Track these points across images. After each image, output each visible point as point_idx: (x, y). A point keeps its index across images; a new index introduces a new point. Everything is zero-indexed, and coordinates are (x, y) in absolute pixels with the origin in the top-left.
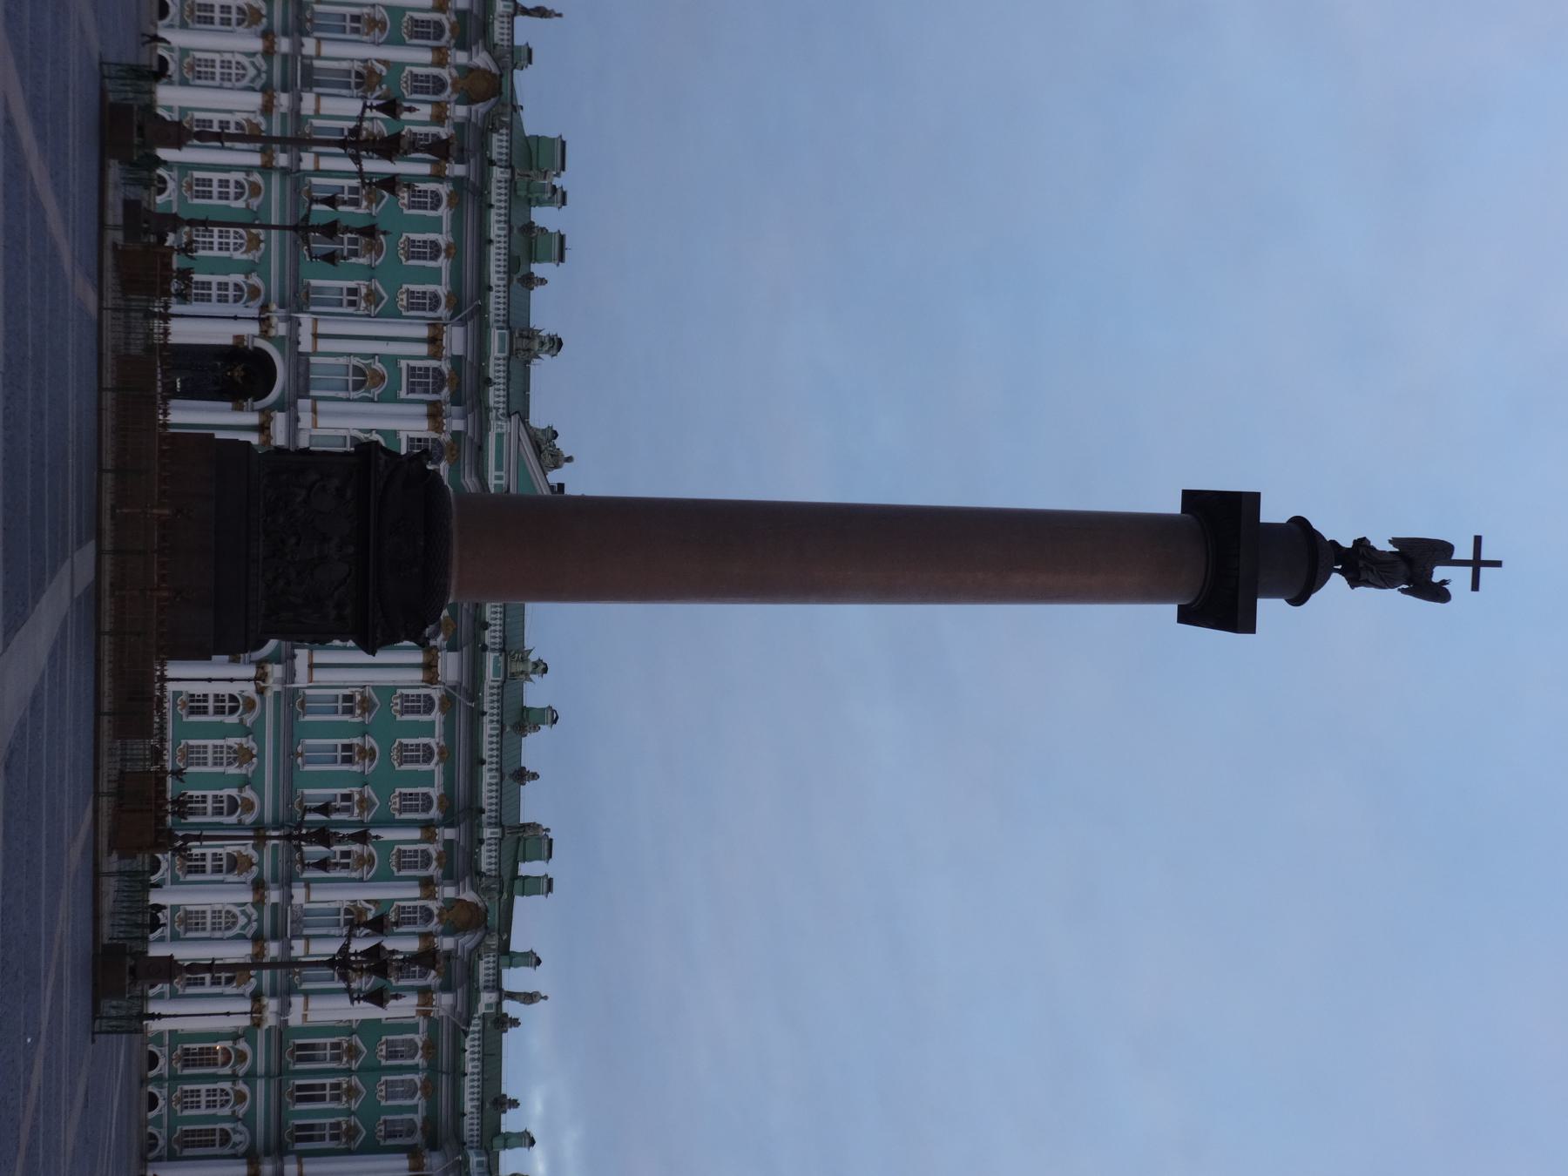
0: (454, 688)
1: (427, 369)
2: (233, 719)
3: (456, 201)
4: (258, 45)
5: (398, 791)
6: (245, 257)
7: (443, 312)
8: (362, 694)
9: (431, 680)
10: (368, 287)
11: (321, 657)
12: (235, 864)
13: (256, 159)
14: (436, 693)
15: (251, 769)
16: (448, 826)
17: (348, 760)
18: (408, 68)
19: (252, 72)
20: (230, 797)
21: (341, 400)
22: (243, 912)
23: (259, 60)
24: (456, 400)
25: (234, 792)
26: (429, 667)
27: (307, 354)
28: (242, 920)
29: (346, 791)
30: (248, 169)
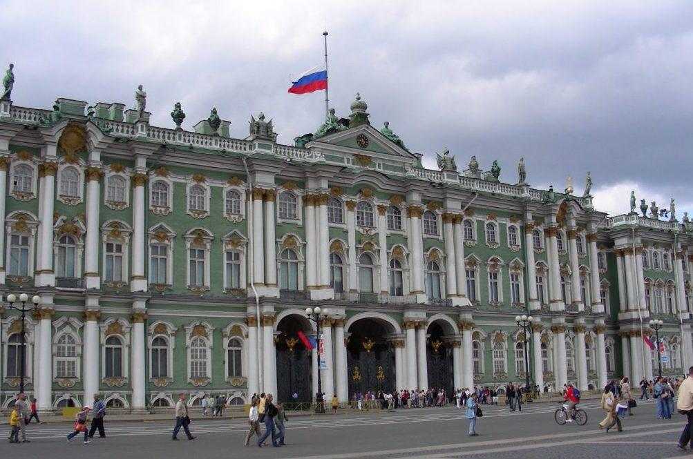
0: (463, 207)
2: (482, 344)
4: (45, 324)
6: (211, 338)
7: (242, 189)
10: (227, 244)
11: (453, 291)
13: (139, 327)
14: (465, 218)
18: (58, 198)
19: (67, 329)
21: (305, 267)
23: (58, 323)
24: (302, 185)
27: (281, 291)
28: (568, 339)
30: (146, 334)
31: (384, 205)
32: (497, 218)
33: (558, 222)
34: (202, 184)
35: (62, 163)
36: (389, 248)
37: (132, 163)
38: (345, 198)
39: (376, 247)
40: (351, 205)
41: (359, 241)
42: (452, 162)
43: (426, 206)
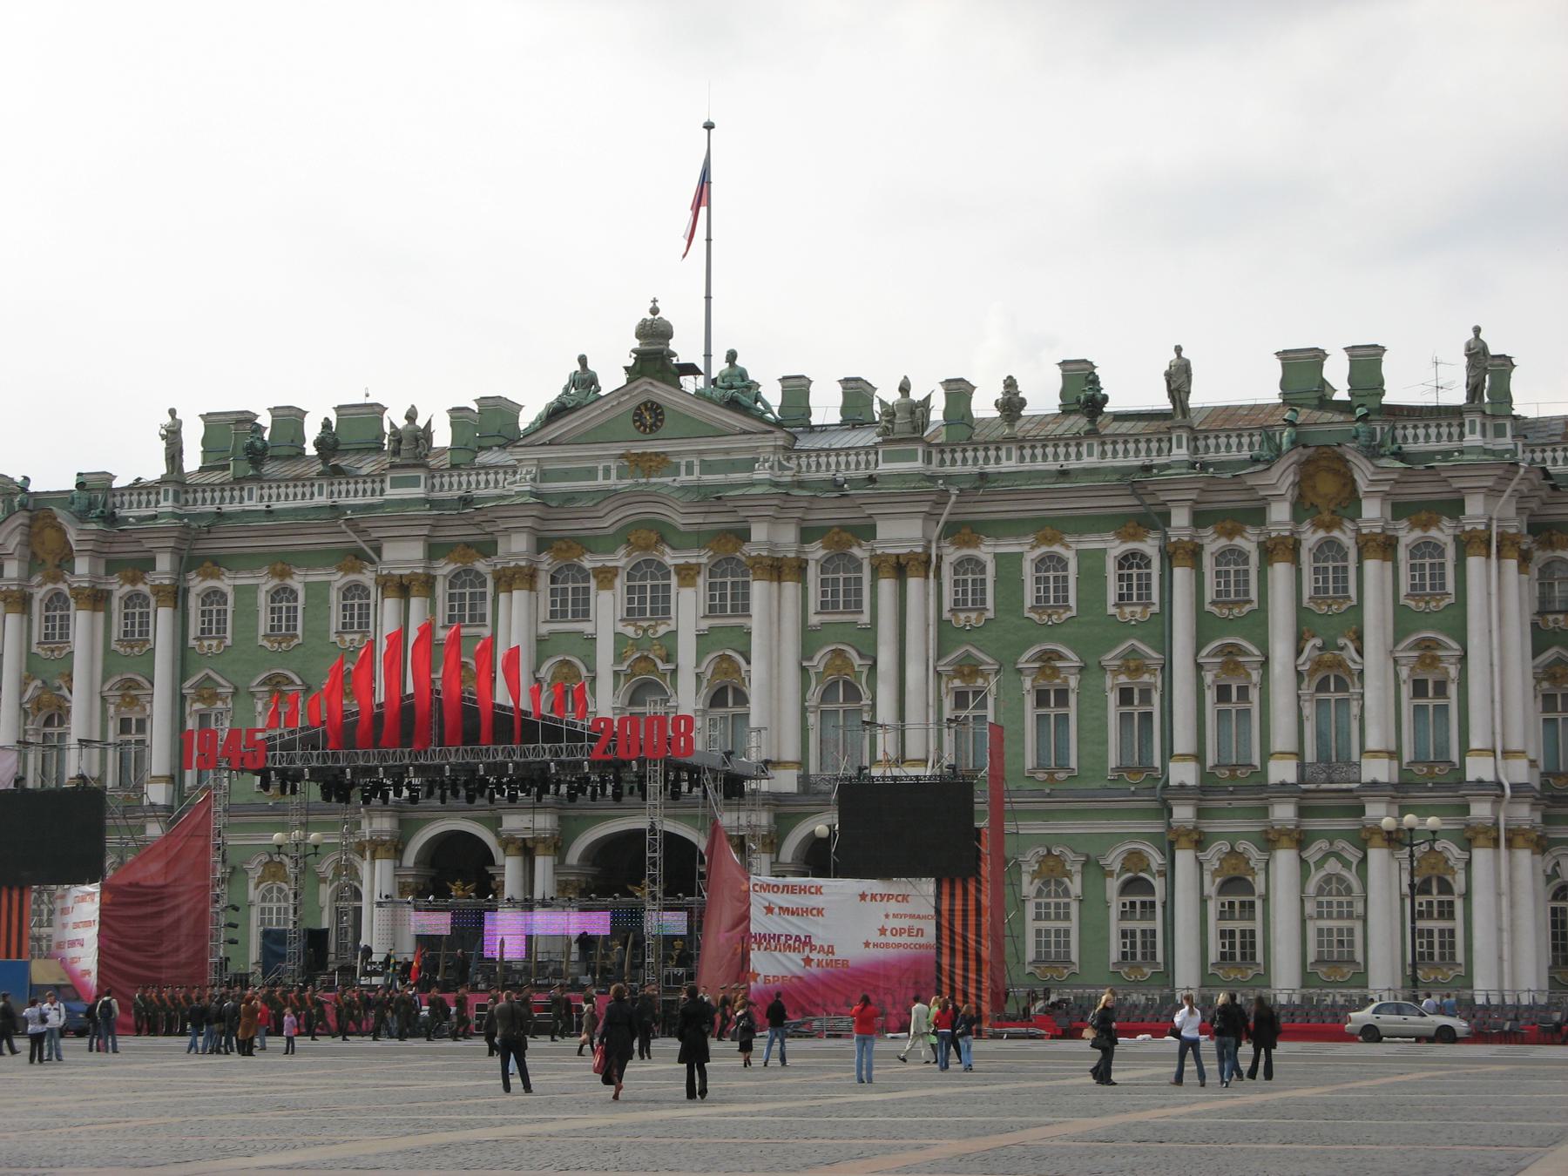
1: (451, 597)
3: (215, 564)
5: (1111, 610)
7: (367, 578)
8: (951, 678)
9: (924, 564)
12: (1235, 883)
15: (1070, 856)
16: (1166, 518)
17: (1062, 696)
20: (1126, 888)
22: (1320, 864)
24: (487, 548)
25: (1113, 885)
26: (900, 569)
28: (1332, 866)
29: (1113, 698)
31: (693, 561)
32: (1068, 539)
33: (1301, 509)
34: (288, 581)
35: (40, 586)
36: (698, 666)
37: (150, 564)
38: (588, 562)
39: (661, 666)
40: (606, 576)
41: (619, 657)
42: (912, 413)
43: (817, 544)
